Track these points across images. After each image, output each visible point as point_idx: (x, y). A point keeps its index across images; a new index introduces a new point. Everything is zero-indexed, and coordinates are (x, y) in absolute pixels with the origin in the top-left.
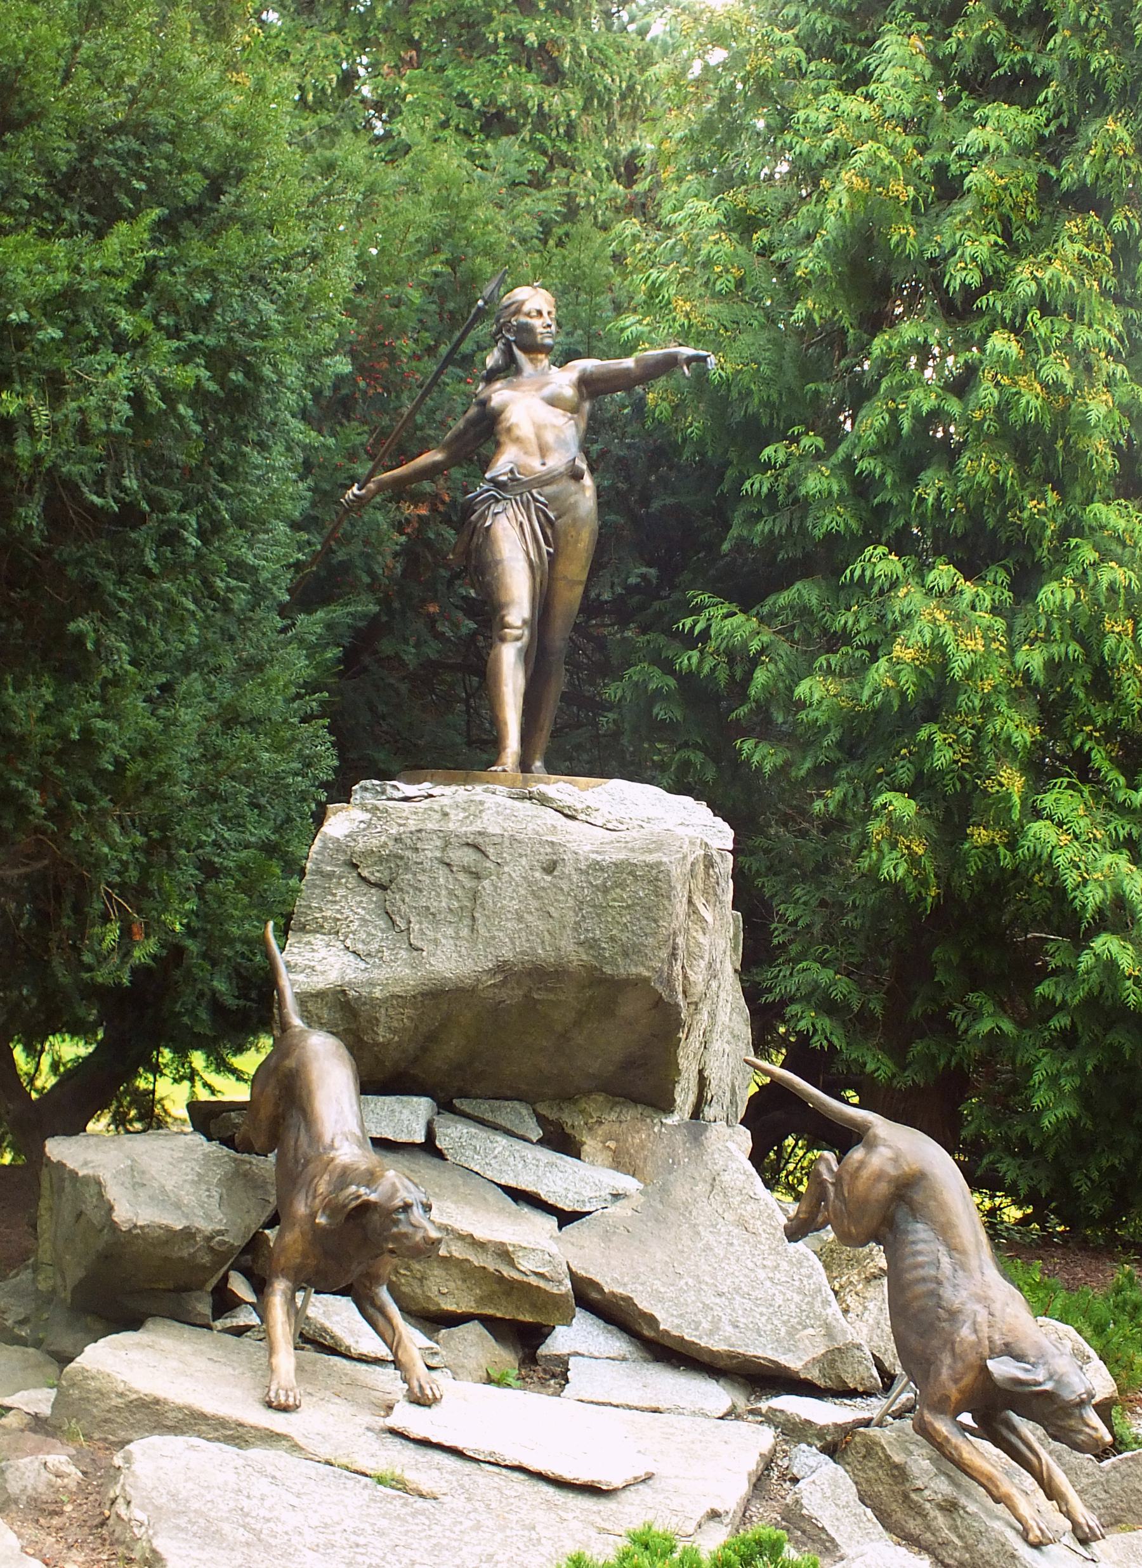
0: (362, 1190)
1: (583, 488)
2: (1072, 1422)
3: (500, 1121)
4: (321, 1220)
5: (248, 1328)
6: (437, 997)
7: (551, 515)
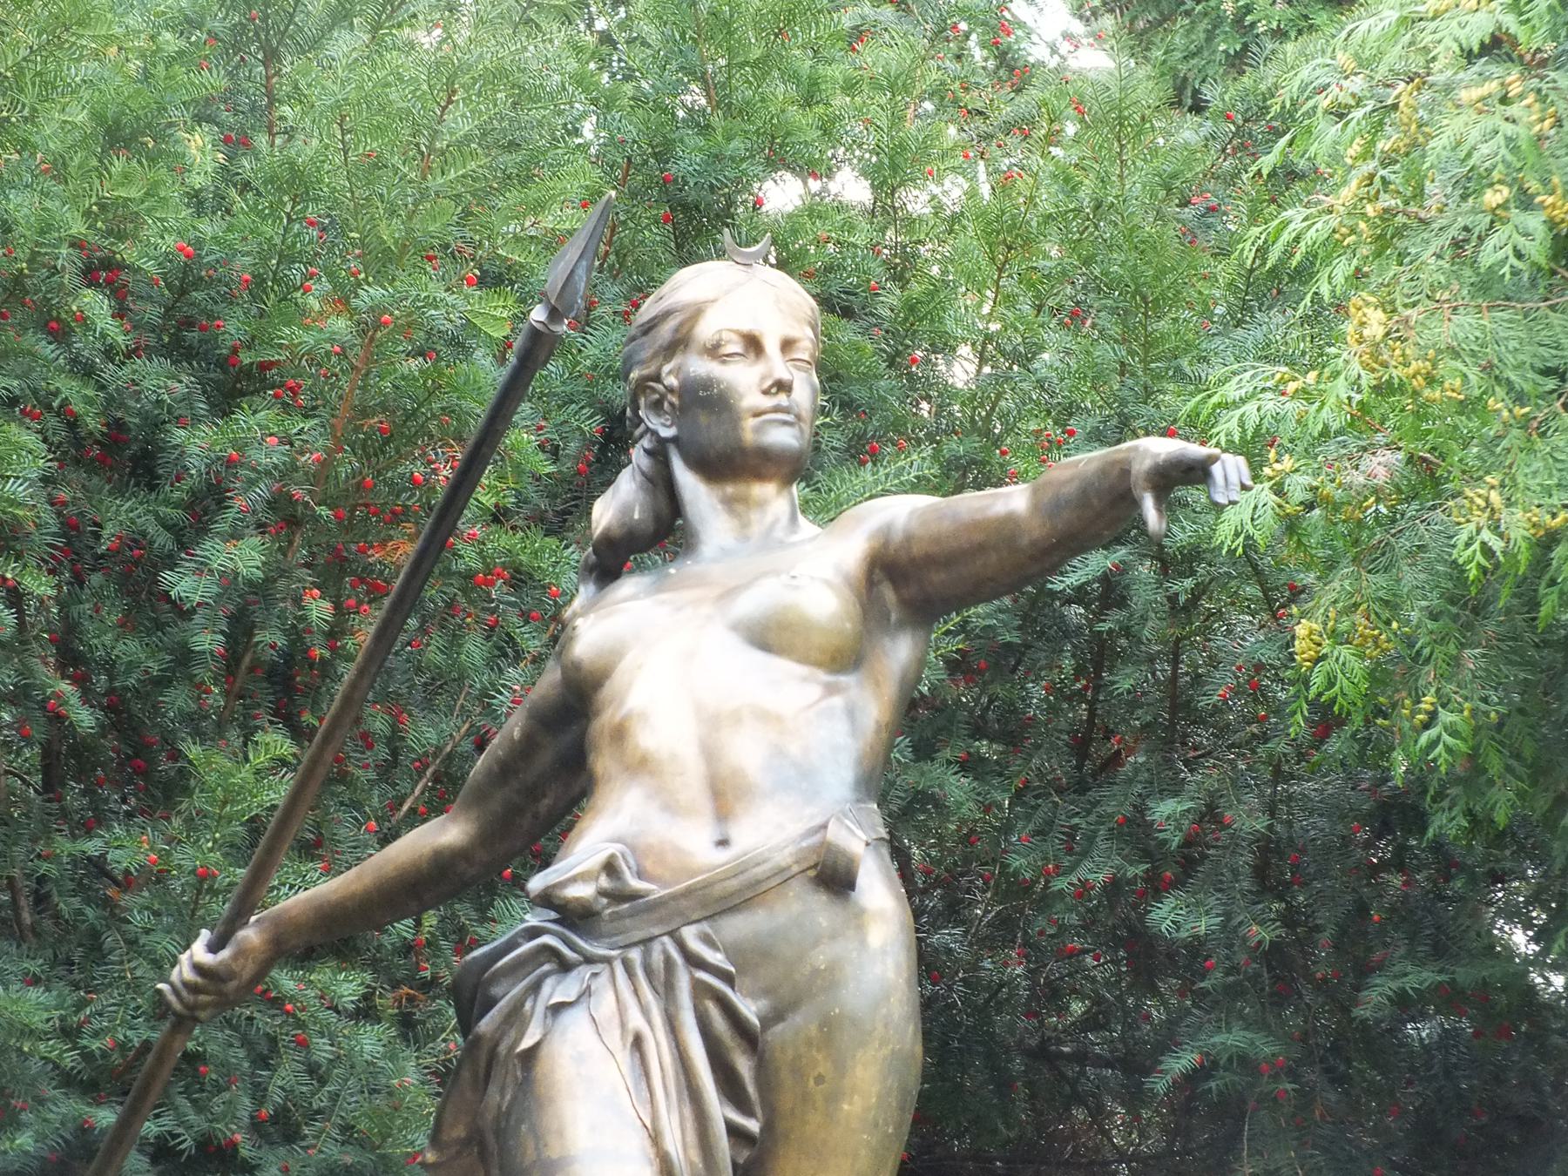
1: (858, 918)
7: (750, 1009)
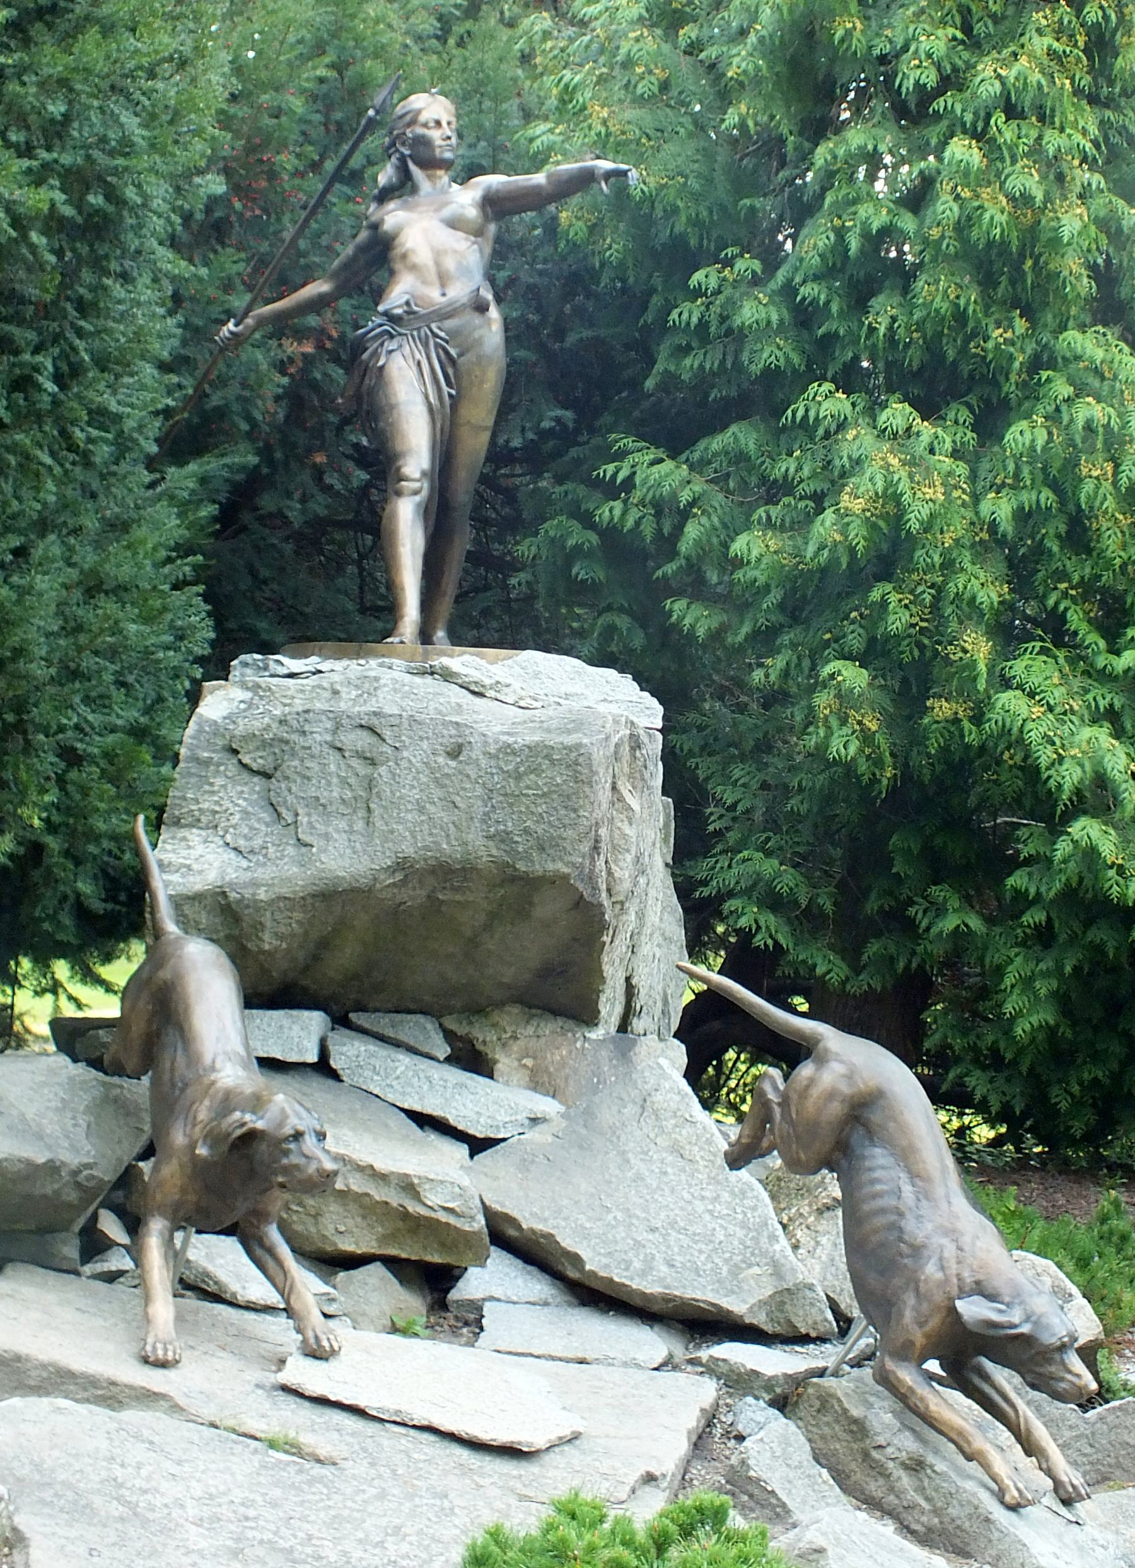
0: (248, 1117)
1: (489, 322)
2: (1053, 1369)
3: (402, 1037)
4: (202, 1151)
5: (121, 1273)
6: (329, 898)
